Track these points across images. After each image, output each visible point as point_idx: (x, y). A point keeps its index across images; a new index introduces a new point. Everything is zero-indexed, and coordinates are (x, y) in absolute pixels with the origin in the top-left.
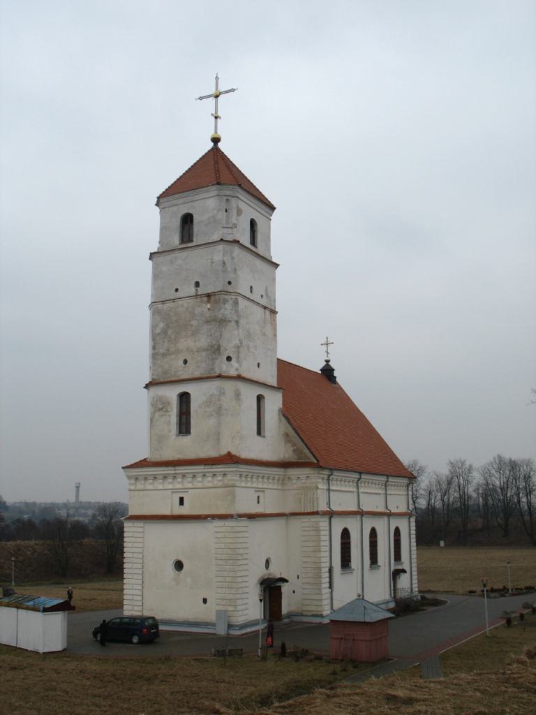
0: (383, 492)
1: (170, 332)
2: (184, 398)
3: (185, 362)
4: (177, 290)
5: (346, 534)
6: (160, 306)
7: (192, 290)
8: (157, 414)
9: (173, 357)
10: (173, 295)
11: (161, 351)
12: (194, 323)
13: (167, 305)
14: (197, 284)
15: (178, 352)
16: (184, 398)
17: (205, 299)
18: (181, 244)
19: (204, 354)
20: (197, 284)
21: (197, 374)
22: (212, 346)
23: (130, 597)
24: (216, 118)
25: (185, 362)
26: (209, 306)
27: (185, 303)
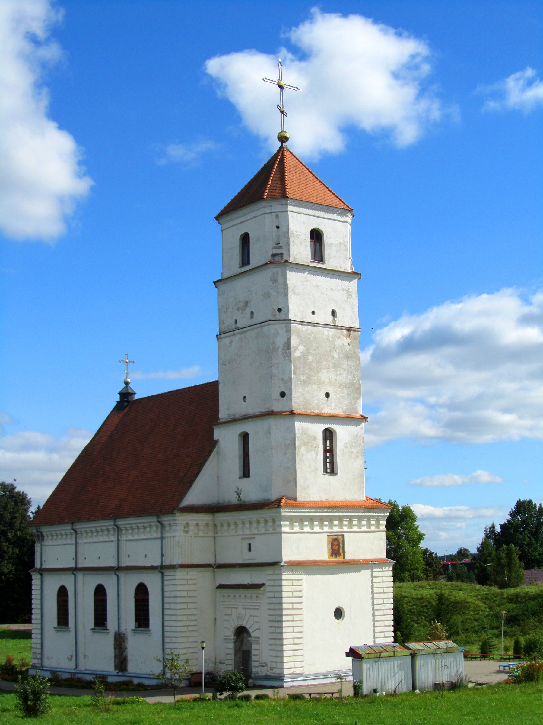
0: (113, 538)
1: (310, 358)
2: (329, 435)
3: (327, 395)
4: (313, 313)
5: (62, 592)
6: (299, 326)
7: (329, 319)
8: (303, 449)
9: (315, 387)
10: (311, 318)
11: (302, 378)
12: (335, 355)
13: (305, 328)
14: (333, 313)
15: (320, 383)
16: (329, 435)
17: (345, 332)
18: (311, 262)
19: (345, 391)
20: (333, 313)
21: (339, 411)
22: (353, 384)
23: (291, 653)
24: (282, 112)
25: (327, 395)
26: (348, 340)
27: (325, 331)
